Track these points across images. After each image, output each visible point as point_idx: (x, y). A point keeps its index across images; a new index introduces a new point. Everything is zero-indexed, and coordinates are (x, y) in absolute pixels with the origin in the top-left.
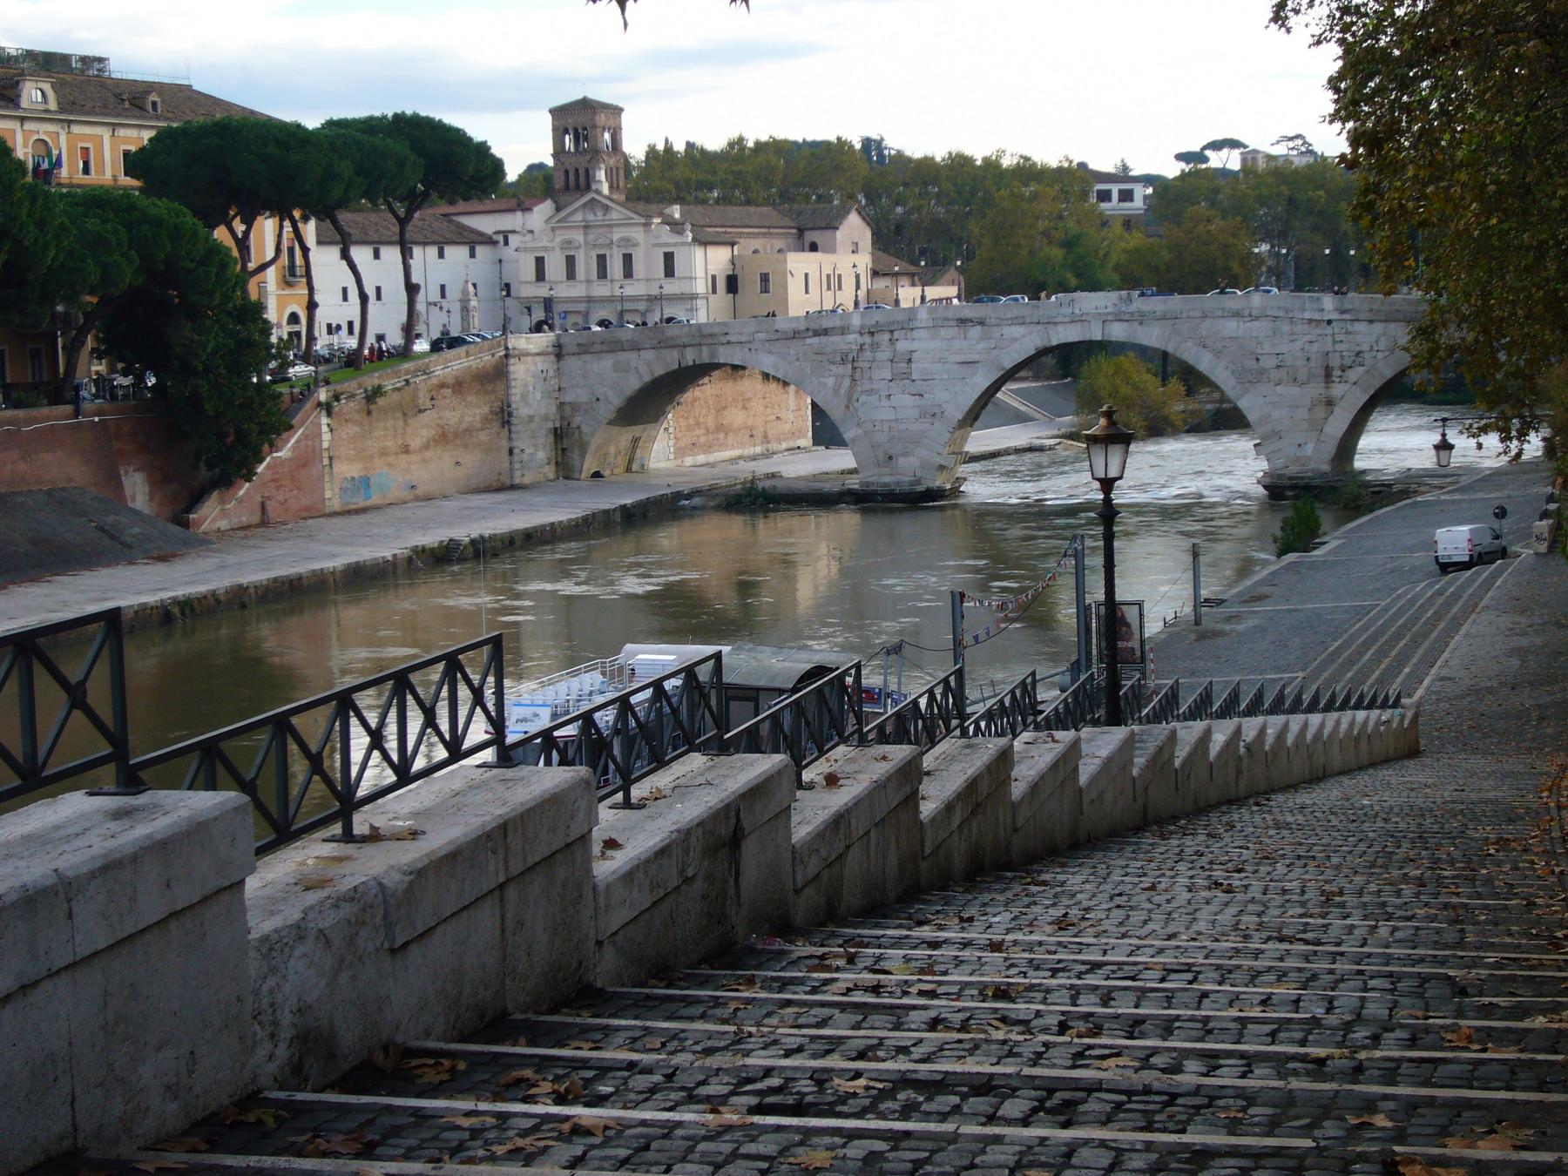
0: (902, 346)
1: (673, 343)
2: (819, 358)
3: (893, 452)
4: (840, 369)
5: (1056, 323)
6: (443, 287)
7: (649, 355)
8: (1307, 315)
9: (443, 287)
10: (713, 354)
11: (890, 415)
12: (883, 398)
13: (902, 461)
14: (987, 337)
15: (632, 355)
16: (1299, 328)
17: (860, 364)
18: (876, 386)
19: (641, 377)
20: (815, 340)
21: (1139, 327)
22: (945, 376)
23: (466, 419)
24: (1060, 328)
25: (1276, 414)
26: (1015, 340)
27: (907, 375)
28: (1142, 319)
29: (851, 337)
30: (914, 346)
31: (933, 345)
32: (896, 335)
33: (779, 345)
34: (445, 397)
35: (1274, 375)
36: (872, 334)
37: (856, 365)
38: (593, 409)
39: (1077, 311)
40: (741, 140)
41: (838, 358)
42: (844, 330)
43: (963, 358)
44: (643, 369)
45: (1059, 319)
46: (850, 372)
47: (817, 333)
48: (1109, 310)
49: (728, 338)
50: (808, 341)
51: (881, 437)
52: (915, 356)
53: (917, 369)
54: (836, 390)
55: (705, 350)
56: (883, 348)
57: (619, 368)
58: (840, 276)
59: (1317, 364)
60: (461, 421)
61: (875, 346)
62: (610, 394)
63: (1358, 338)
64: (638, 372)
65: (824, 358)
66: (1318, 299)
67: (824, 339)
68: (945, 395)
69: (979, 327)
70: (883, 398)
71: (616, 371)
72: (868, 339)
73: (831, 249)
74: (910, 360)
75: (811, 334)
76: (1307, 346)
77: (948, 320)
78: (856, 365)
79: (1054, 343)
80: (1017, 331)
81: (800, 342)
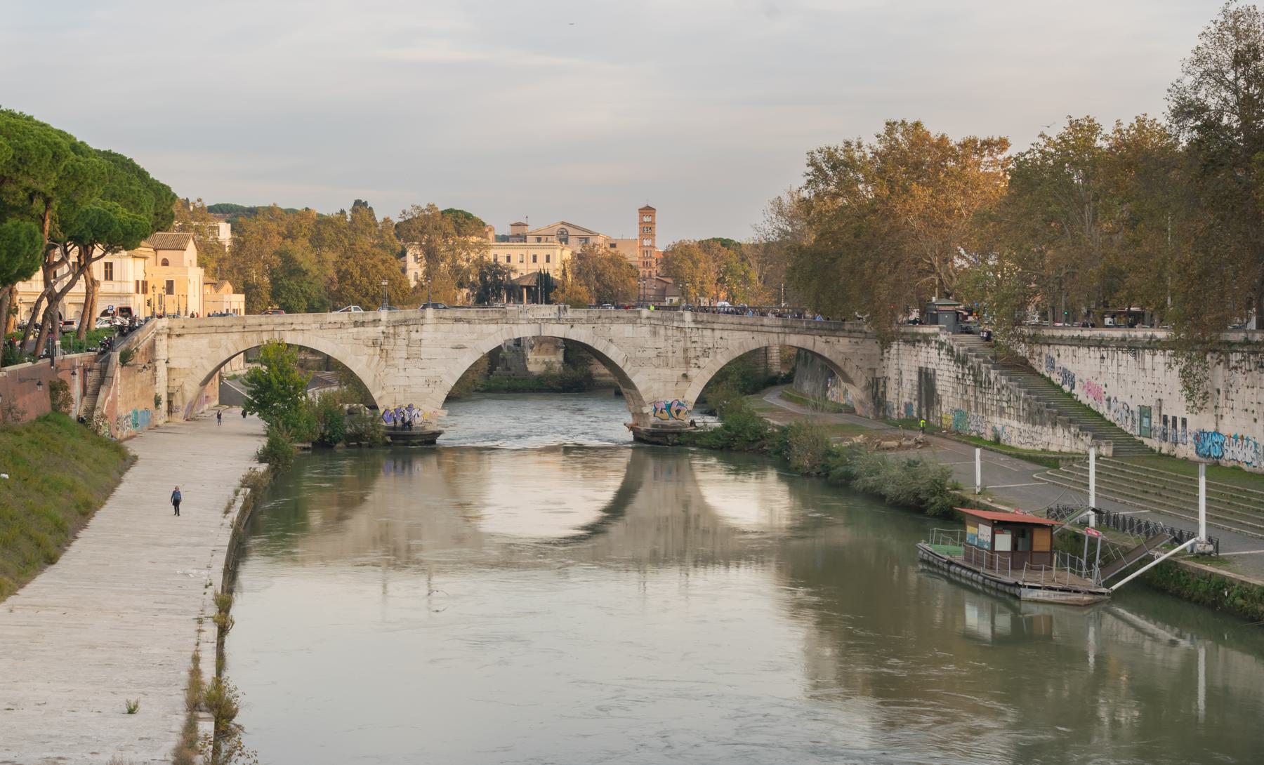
1: (254, 329)
2: (357, 342)
4: (371, 351)
5: (518, 324)
7: (236, 337)
8: (675, 324)
11: (404, 382)
15: (224, 336)
16: (670, 332)
17: (386, 347)
19: (229, 351)
20: (356, 329)
22: (444, 357)
24: (520, 326)
25: (656, 386)
26: (490, 334)
28: (572, 323)
29: (382, 328)
35: (656, 361)
36: (394, 326)
37: (383, 347)
38: (193, 374)
39: (531, 317)
40: (1093, 129)
41: (370, 343)
44: (230, 346)
45: (520, 322)
48: (552, 316)
49: (294, 326)
50: (350, 330)
53: (426, 352)
54: (368, 365)
55: (276, 335)
59: (680, 354)
63: (706, 340)
64: (227, 348)
65: (361, 342)
66: (682, 314)
67: (361, 329)
69: (467, 325)
70: (401, 370)
72: (391, 331)
76: (675, 344)
78: (383, 347)
80: (493, 328)
81: (345, 331)
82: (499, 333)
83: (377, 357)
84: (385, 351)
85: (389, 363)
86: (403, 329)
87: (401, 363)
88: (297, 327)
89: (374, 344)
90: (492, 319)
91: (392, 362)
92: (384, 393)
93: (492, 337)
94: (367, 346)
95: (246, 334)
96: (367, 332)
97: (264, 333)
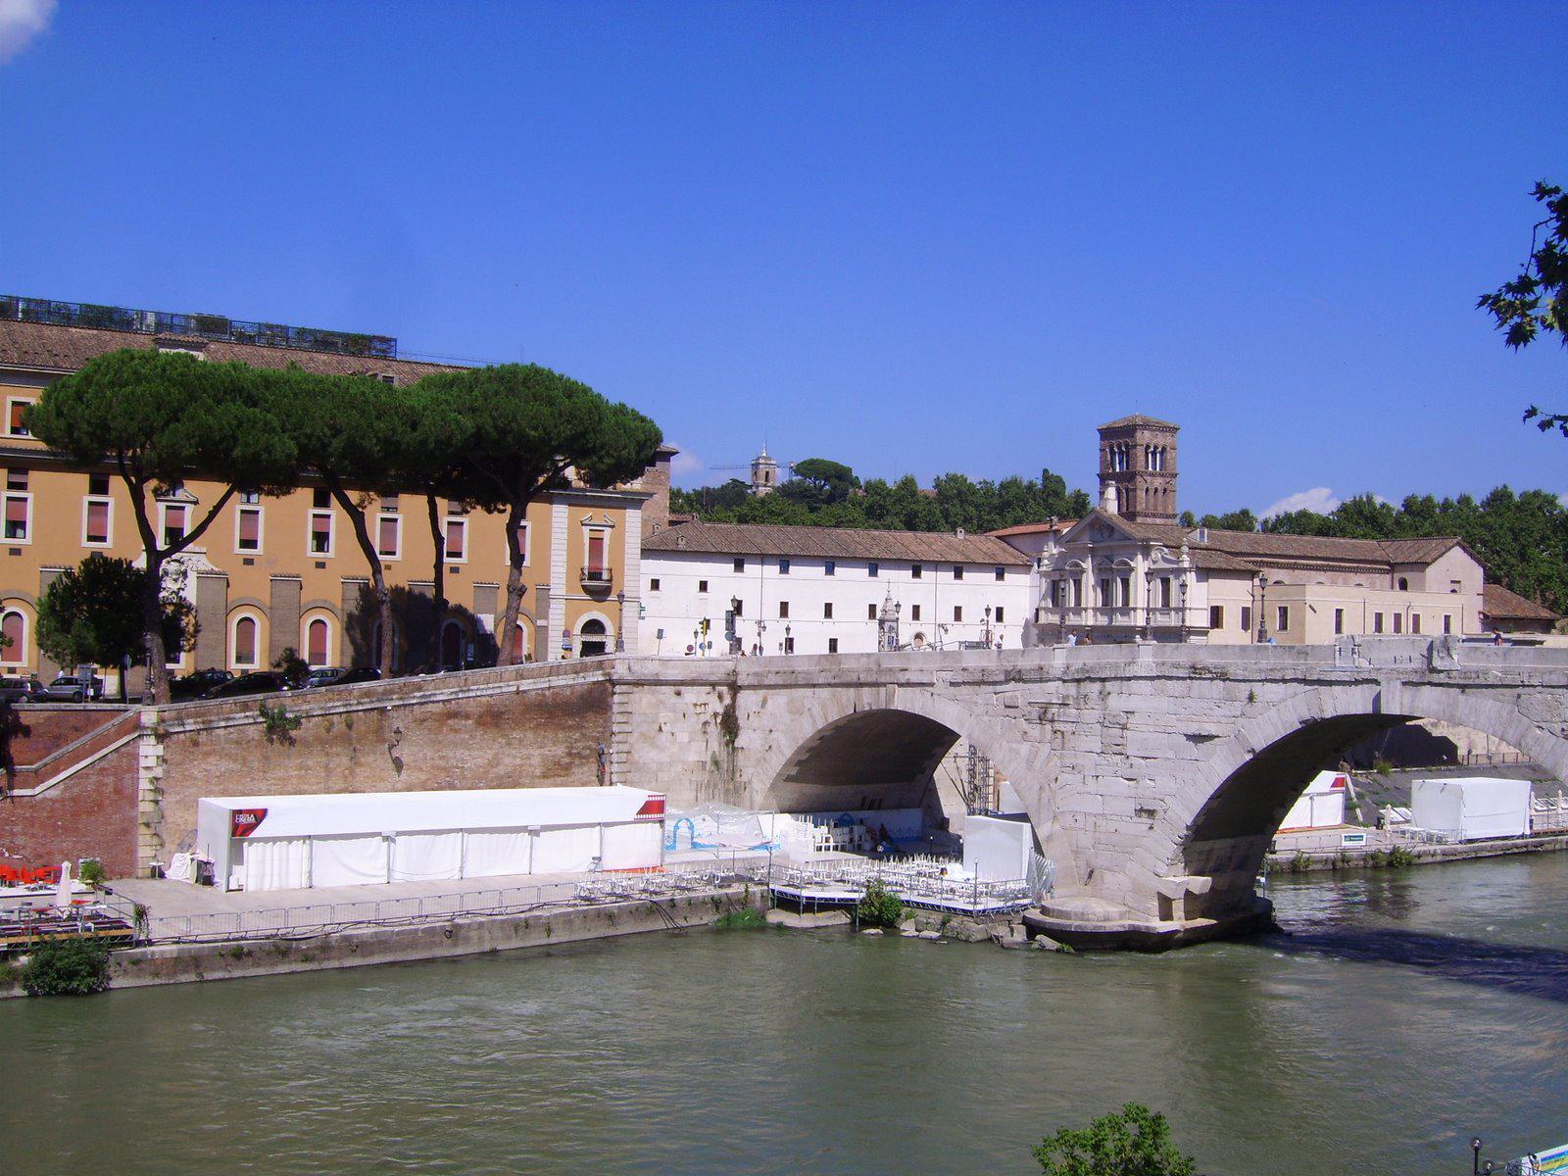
0: (1116, 703)
3: (1097, 862)
4: (1035, 731)
5: (1330, 683)
10: (890, 697)
11: (1092, 805)
12: (1089, 780)
13: (1108, 876)
14: (1231, 699)
18: (1080, 761)
21: (1462, 698)
22: (1171, 754)
23: (507, 760)
30: (1132, 703)
39: (1364, 664)
41: (1035, 715)
43: (1194, 729)
44: (817, 711)
46: (1049, 735)
51: (1085, 840)
53: (1134, 742)
54: (1030, 763)
56: (1091, 704)
57: (796, 710)
58: (1416, 618)
60: (494, 763)
62: (783, 741)
68: (1165, 784)
70: (1089, 780)
71: (791, 712)
73: (1421, 588)
78: (1057, 726)
79: (1328, 714)
82: (1289, 702)
83: (1045, 749)
84: (1059, 735)
85: (1068, 762)
88: (914, 679)
90: (1272, 670)
91: (1074, 761)
92: (1057, 827)
93: (1273, 712)
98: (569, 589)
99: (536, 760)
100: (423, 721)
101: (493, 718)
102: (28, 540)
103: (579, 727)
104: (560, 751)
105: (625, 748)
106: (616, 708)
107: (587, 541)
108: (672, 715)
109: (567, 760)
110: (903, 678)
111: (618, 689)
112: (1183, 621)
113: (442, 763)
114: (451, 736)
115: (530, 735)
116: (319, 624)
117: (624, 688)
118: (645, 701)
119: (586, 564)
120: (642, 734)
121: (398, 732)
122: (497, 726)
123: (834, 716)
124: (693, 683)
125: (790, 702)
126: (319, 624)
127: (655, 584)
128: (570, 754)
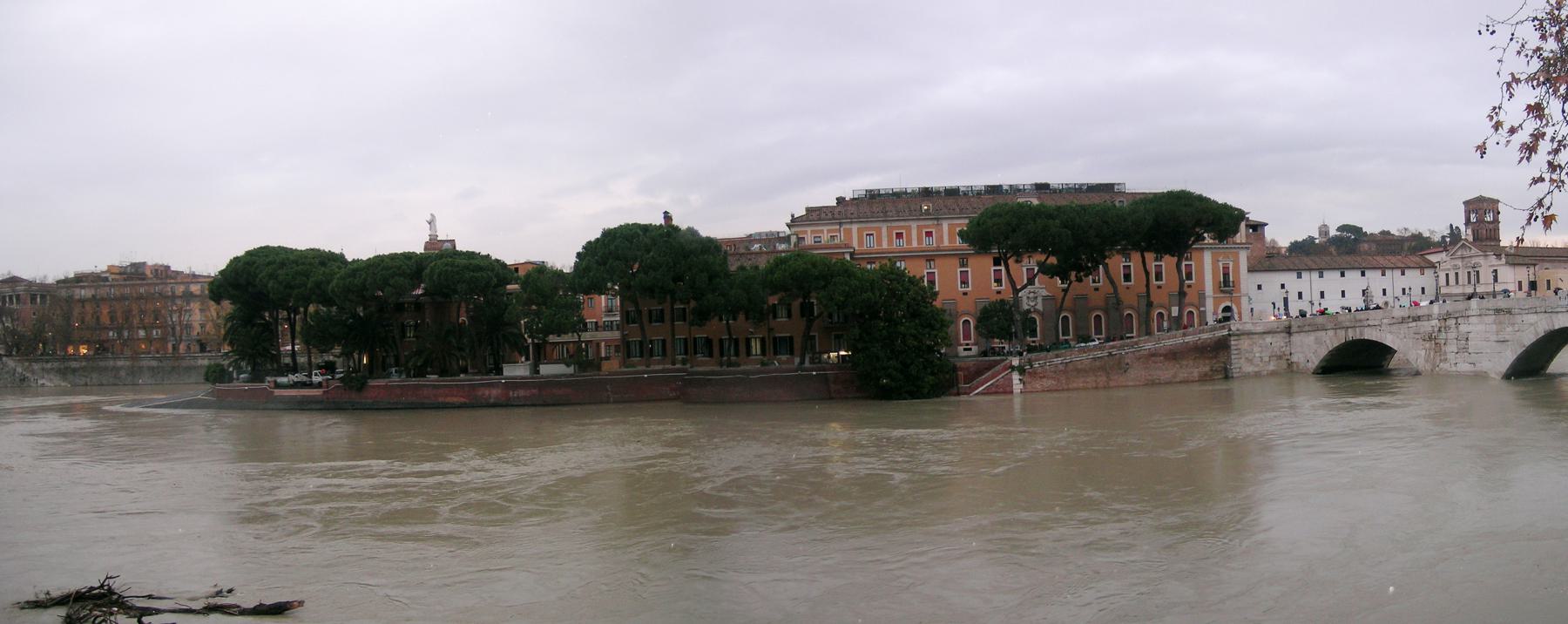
2: (1417, 336)
6: (1423, 289)
7: (1331, 333)
9: (1423, 289)
10: (1361, 334)
15: (1323, 333)
20: (1414, 324)
27: (1465, 349)
29: (1435, 322)
30: (1470, 328)
31: (1481, 327)
32: (1459, 320)
33: (1395, 327)
34: (1156, 363)
37: (1437, 341)
42: (1429, 317)
44: (1328, 342)
47: (1414, 320)
50: (1410, 325)
52: (1470, 336)
56: (1452, 330)
57: (1318, 341)
61: (1447, 328)
65: (1418, 336)
74: (1467, 339)
75: (1411, 320)
77: (1489, 310)
78: (1437, 341)
86: (1452, 322)
87: (1451, 356)
89: (1430, 339)
94: (1424, 340)
95: (1338, 331)
96: (1423, 326)
97: (1350, 330)
98: (1214, 293)
99: (1196, 374)
100: (1140, 359)
101: (1173, 355)
102: (970, 289)
103: (1216, 357)
104: (1207, 369)
105: (1239, 366)
106: (1232, 348)
107: (1221, 269)
108: (1260, 349)
109: (1210, 373)
110: (1366, 323)
111: (1232, 338)
112: (1475, 289)
113: (1150, 378)
114: (1153, 365)
115: (1191, 362)
116: (1098, 317)
117: (1236, 338)
118: (1246, 343)
119: (1222, 280)
120: (1247, 358)
121: (1128, 364)
122: (1175, 359)
123: (1336, 345)
124: (1269, 333)
125: (1316, 339)
126: (1065, 318)
127: (1259, 287)
128: (1212, 370)
